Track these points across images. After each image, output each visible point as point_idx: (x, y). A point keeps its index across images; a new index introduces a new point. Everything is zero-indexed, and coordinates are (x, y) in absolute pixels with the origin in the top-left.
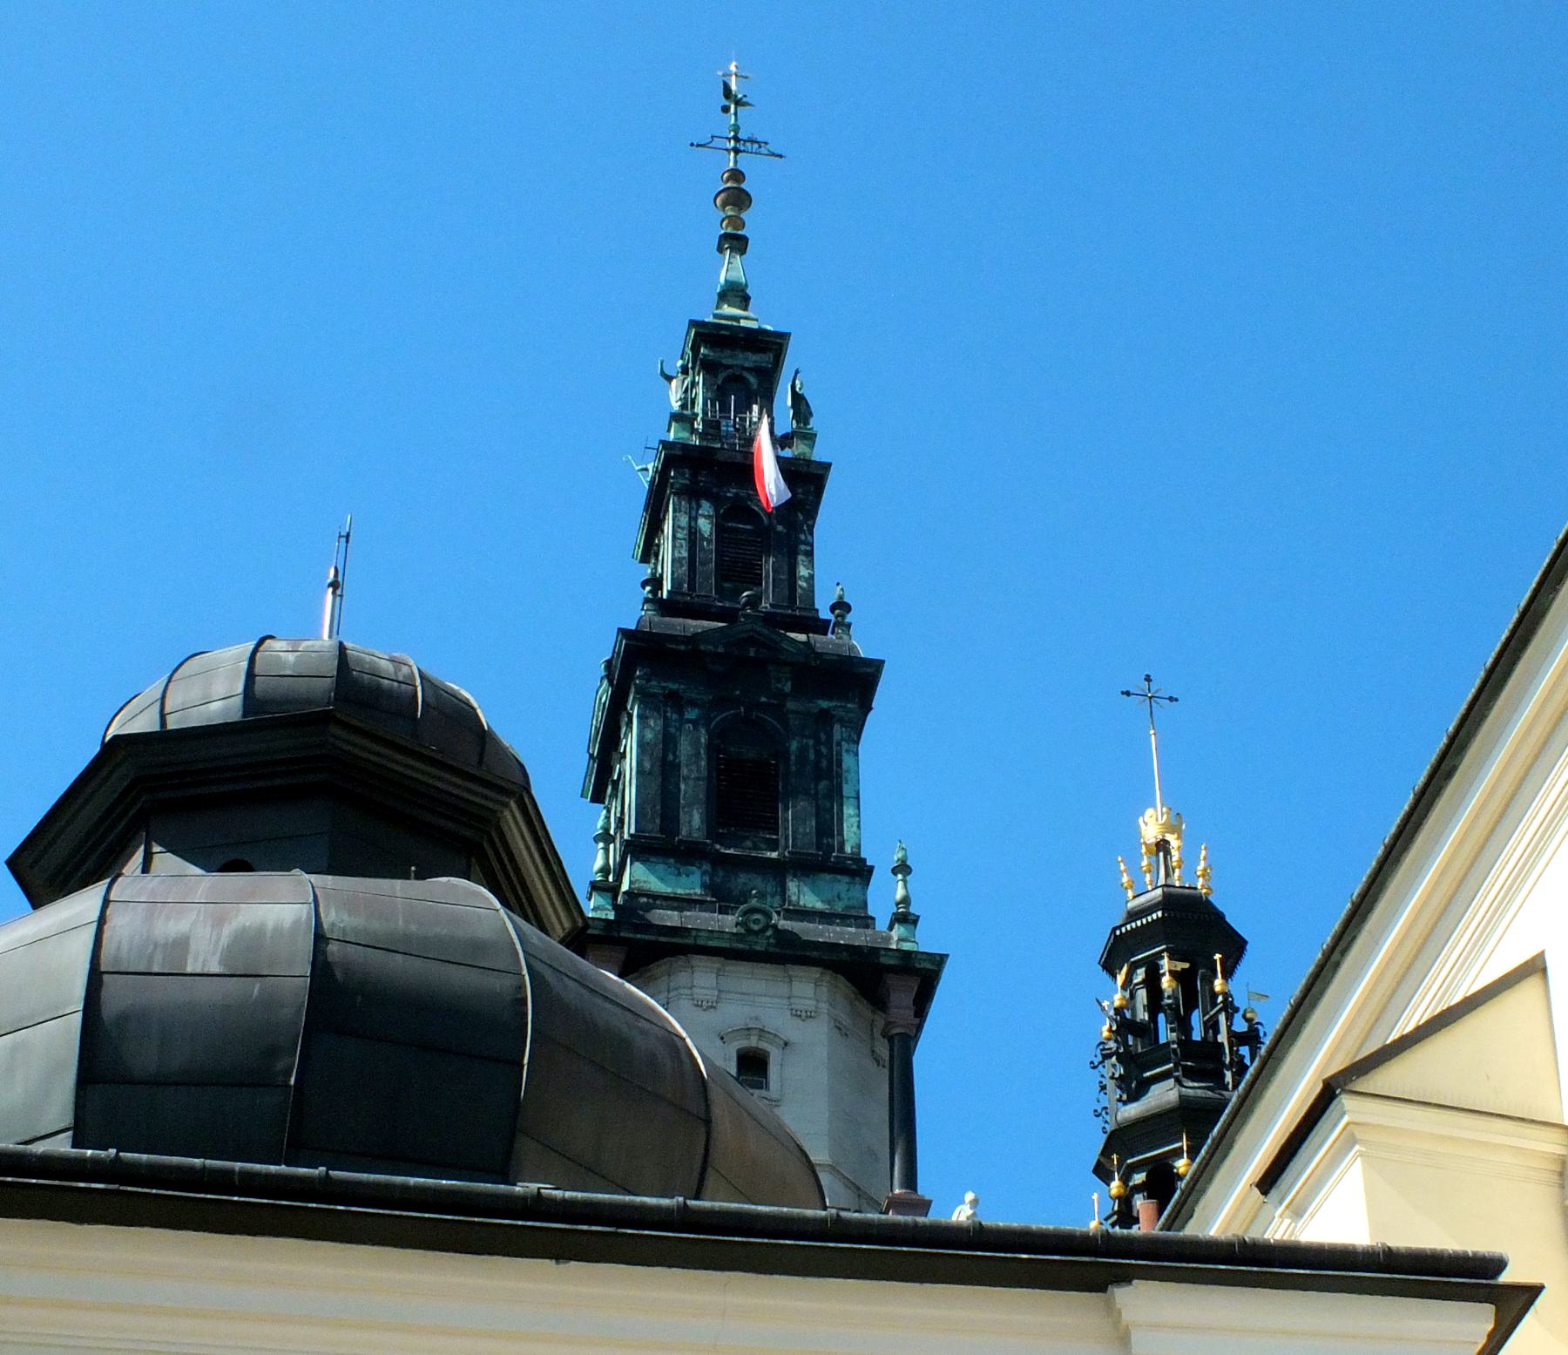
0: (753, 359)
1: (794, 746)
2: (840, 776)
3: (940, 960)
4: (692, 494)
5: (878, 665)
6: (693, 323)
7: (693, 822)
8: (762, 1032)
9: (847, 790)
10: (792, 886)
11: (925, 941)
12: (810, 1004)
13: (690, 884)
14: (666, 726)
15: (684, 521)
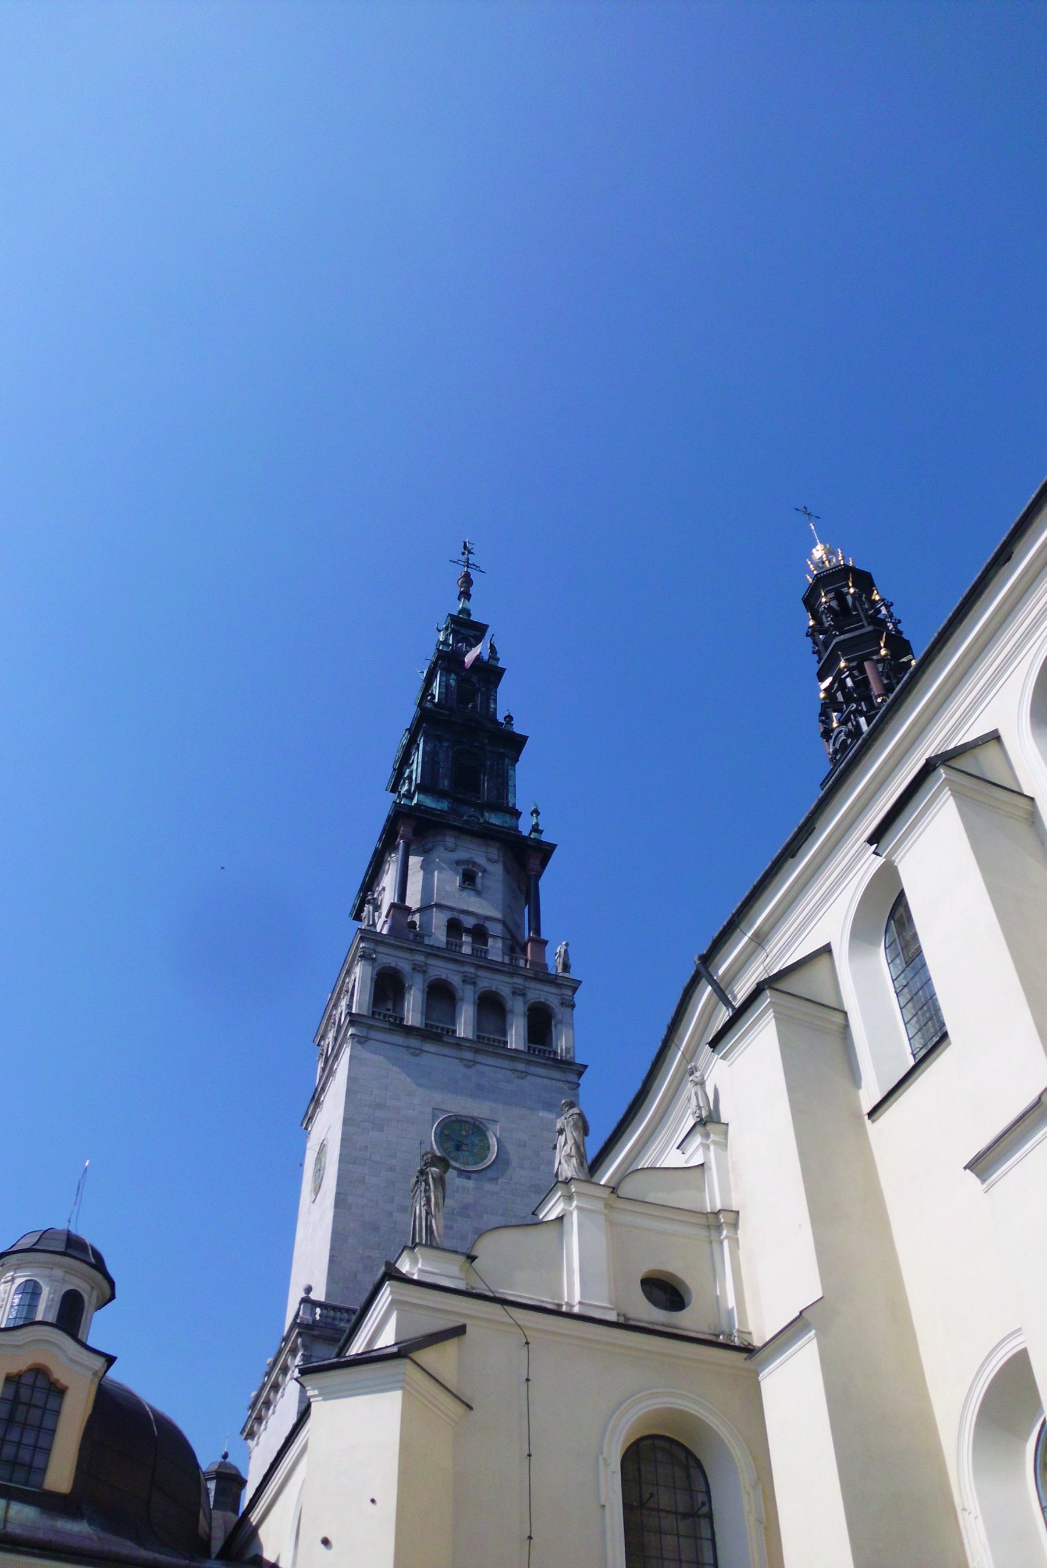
0: (472, 633)
1: (489, 763)
2: (507, 777)
3: (554, 846)
4: (447, 672)
5: (526, 738)
6: (450, 615)
7: (445, 784)
8: (474, 863)
9: (510, 783)
10: (487, 815)
11: (544, 838)
12: (496, 857)
13: (444, 805)
14: (435, 747)
15: (444, 679)
